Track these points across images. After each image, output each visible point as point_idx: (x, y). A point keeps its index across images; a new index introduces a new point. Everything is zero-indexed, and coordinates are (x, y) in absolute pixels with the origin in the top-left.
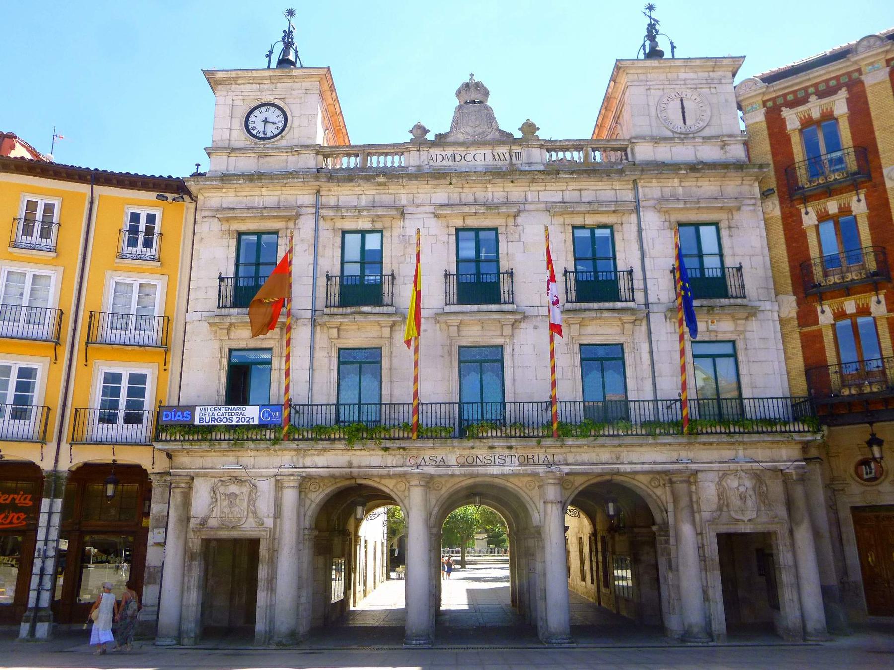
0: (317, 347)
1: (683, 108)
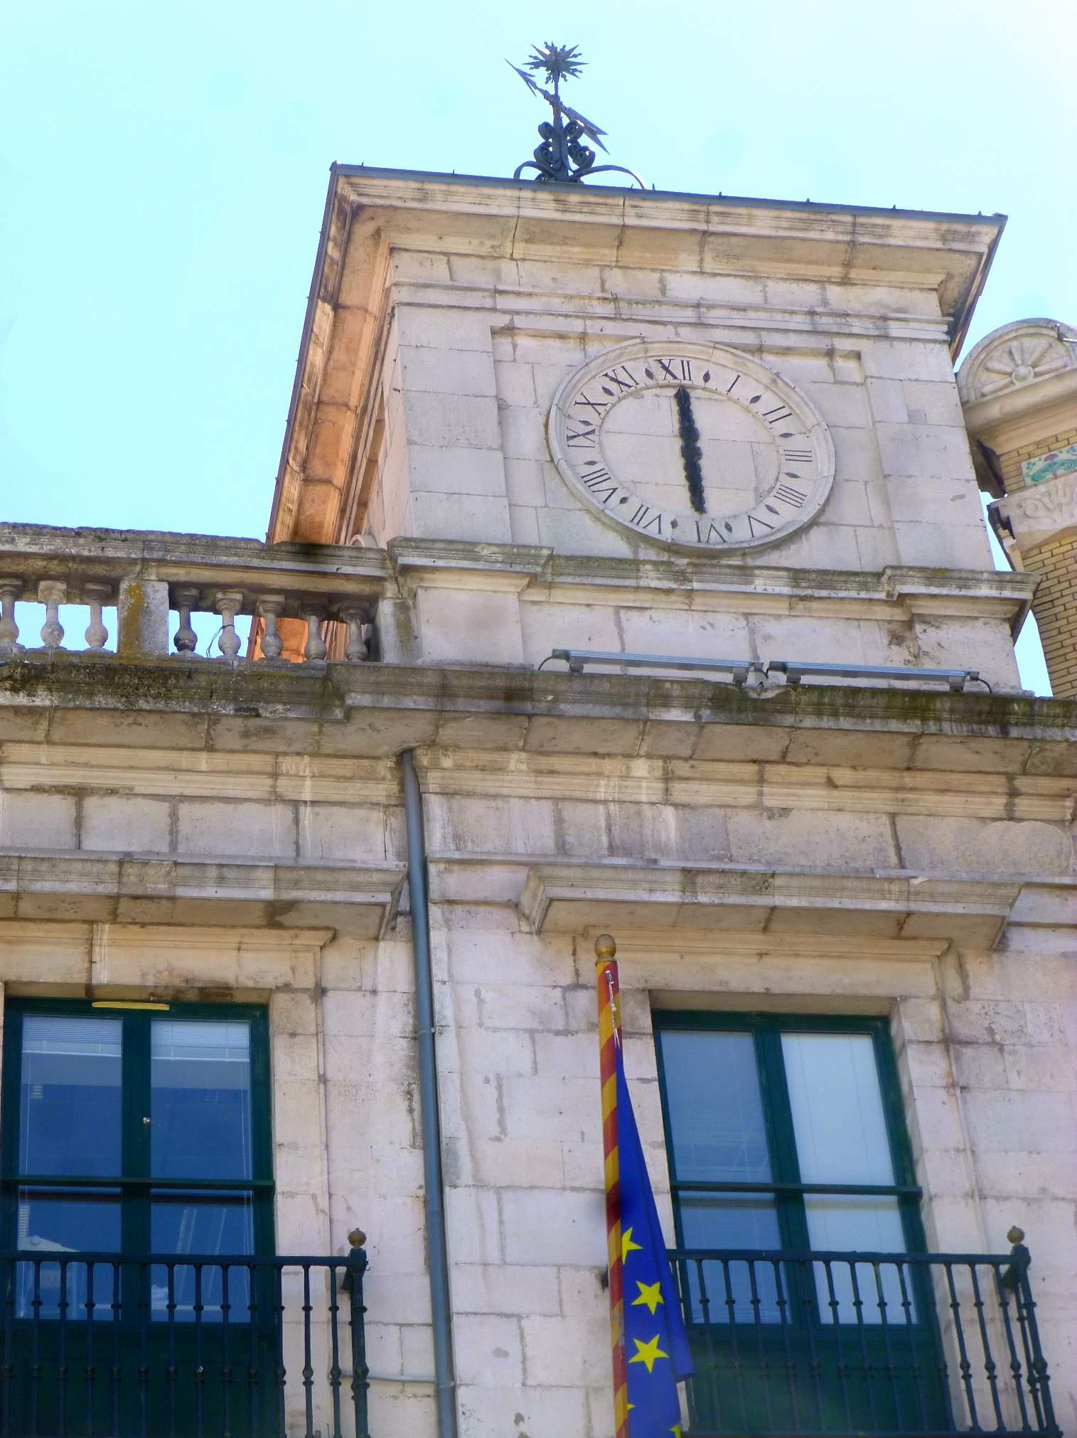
1: (688, 432)
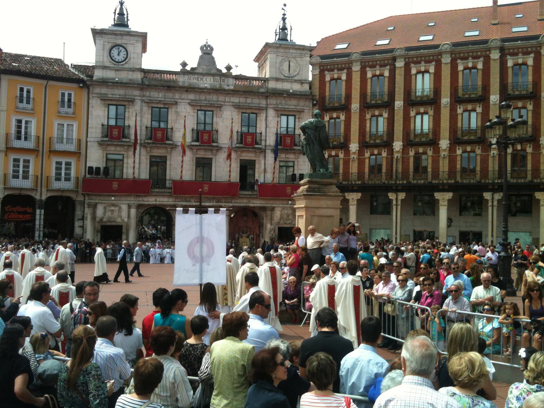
0: (142, 155)
1: (289, 65)
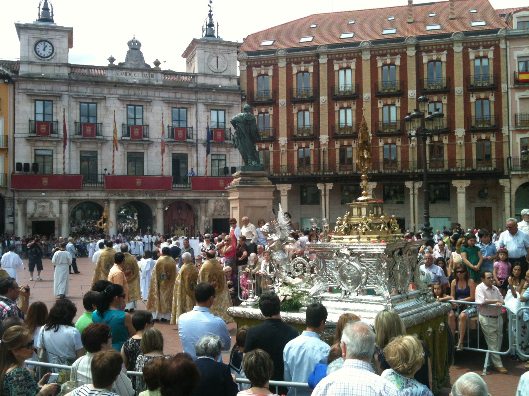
1: (217, 61)
